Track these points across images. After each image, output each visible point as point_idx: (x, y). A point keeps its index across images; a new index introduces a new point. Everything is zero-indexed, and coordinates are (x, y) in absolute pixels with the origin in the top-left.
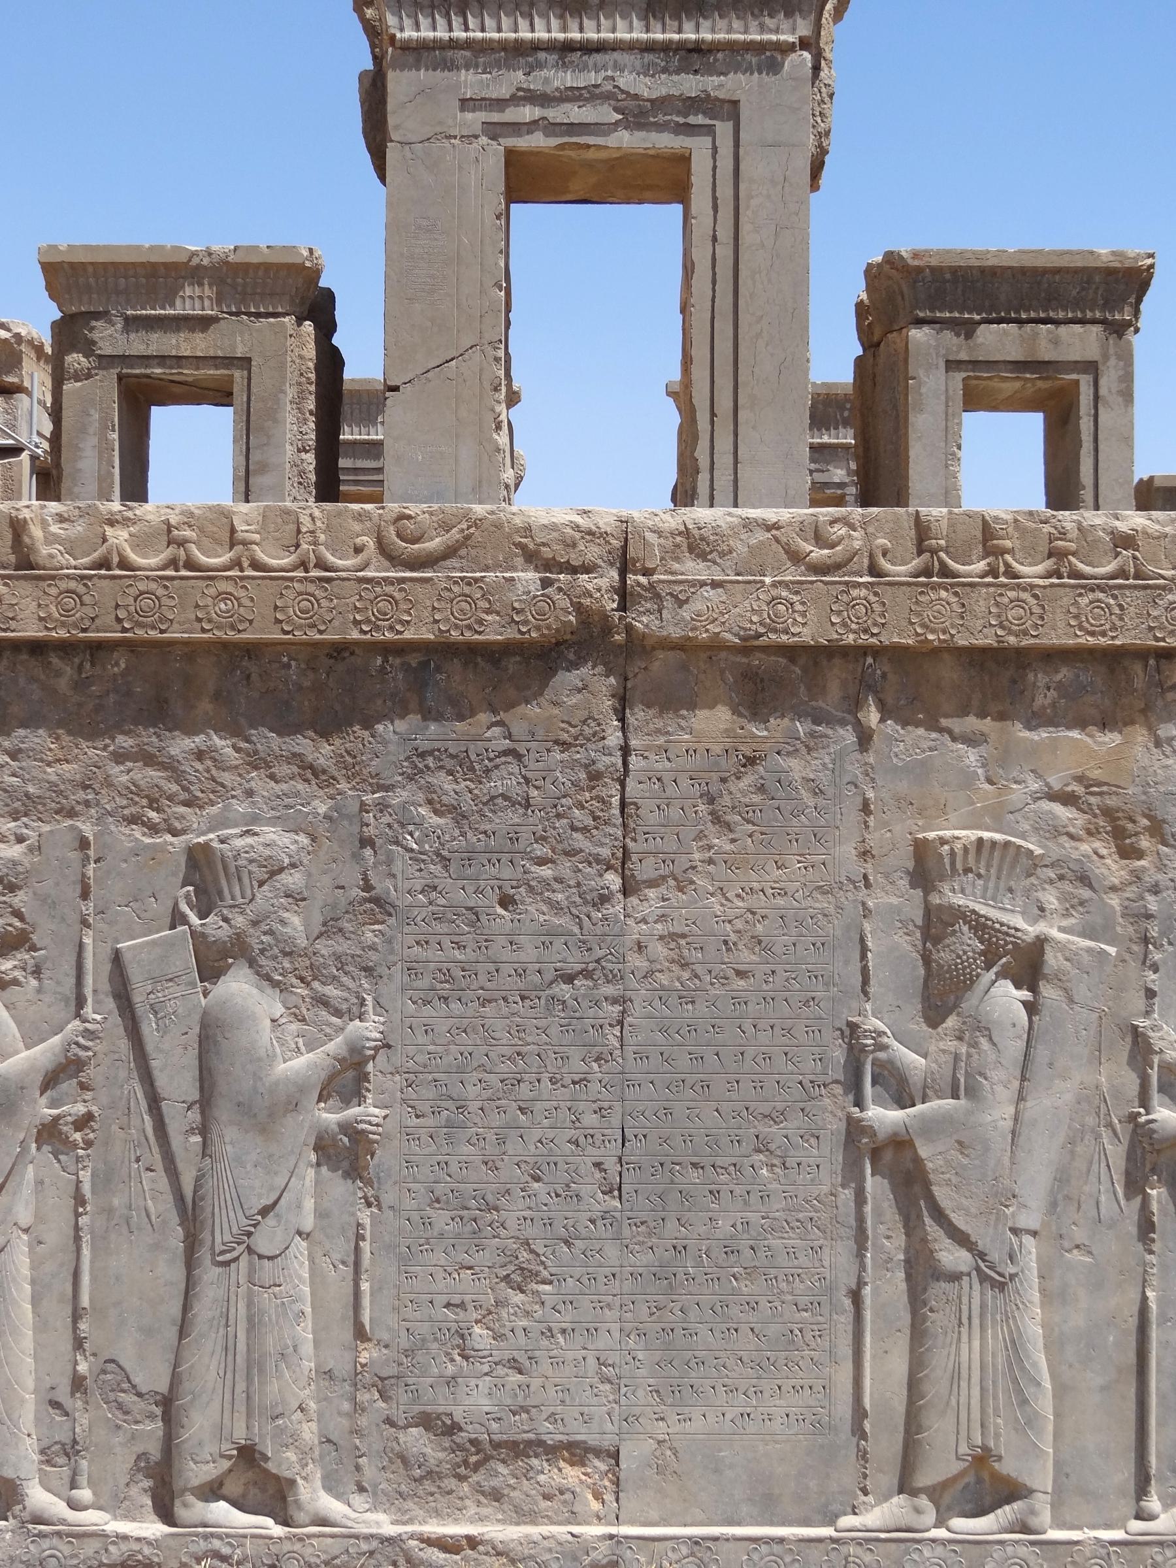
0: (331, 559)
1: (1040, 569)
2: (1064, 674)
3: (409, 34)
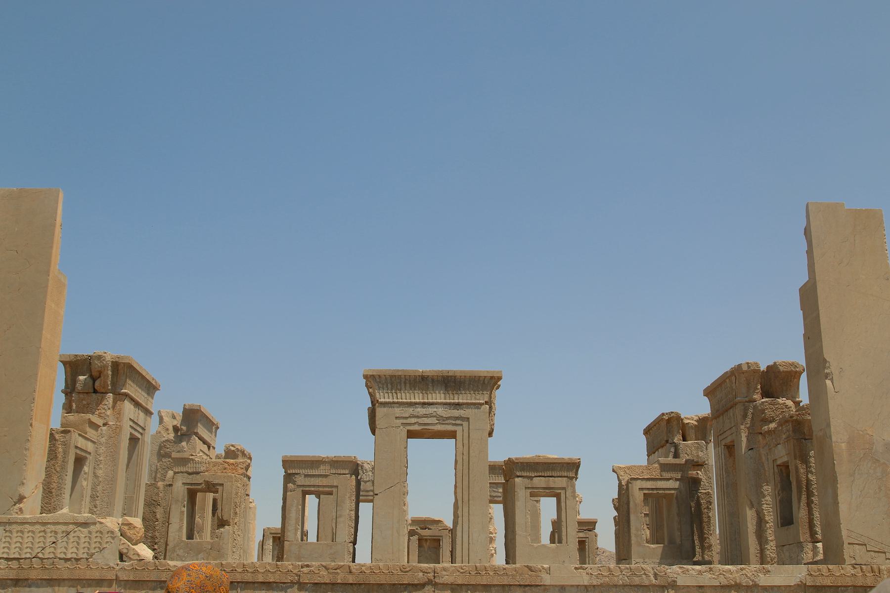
0: (393, 572)
1: (493, 573)
2: (496, 588)
3: (382, 400)
